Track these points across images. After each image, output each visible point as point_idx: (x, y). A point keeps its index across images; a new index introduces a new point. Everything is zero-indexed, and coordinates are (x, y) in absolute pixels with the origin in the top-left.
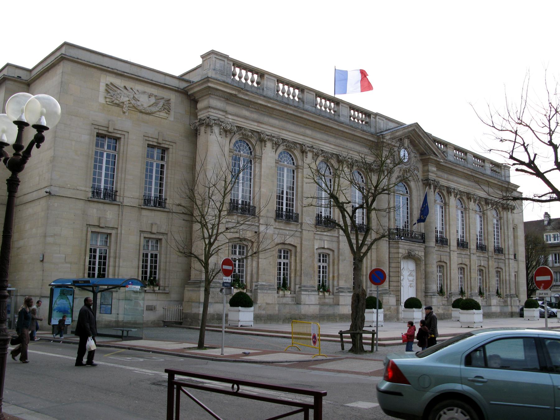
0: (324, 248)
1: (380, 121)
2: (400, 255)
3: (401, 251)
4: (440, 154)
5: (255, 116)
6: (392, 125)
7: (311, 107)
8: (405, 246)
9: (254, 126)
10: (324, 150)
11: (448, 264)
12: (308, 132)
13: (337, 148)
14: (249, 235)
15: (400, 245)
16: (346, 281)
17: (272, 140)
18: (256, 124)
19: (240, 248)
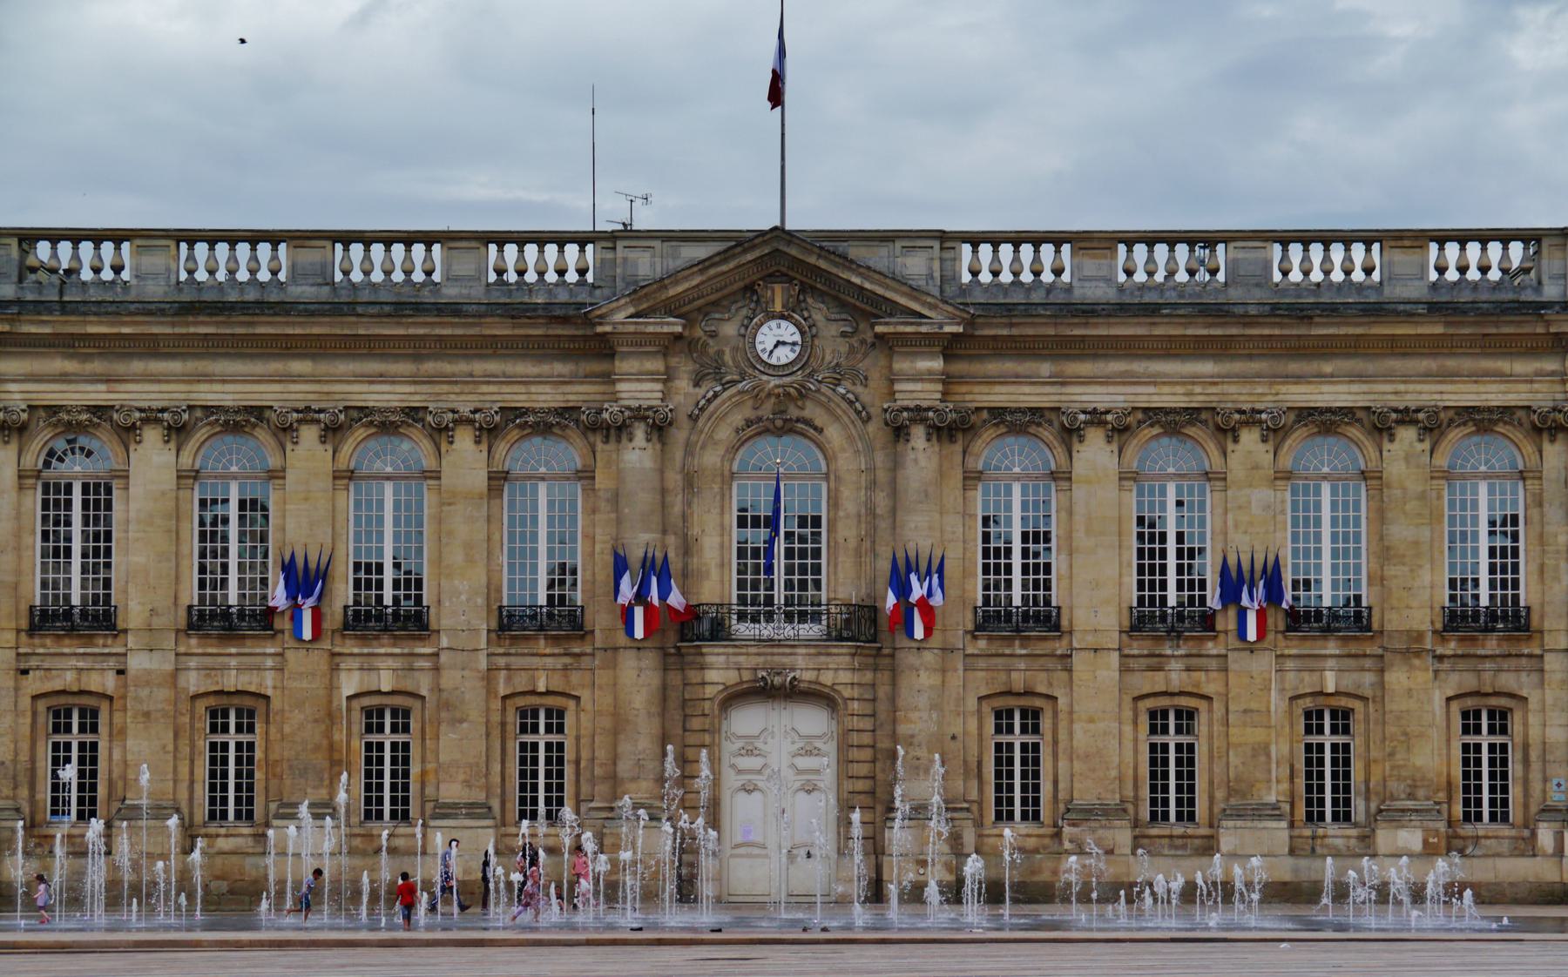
0: (379, 692)
1: (632, 255)
2: (710, 691)
3: (712, 675)
4: (932, 307)
5: (97, 366)
6: (701, 252)
7: (313, 289)
8: (742, 659)
9: (97, 394)
10: (371, 404)
12: (299, 366)
13: (419, 388)
14: (94, 682)
15: (709, 659)
16: (467, 784)
17: (158, 421)
18: (102, 387)
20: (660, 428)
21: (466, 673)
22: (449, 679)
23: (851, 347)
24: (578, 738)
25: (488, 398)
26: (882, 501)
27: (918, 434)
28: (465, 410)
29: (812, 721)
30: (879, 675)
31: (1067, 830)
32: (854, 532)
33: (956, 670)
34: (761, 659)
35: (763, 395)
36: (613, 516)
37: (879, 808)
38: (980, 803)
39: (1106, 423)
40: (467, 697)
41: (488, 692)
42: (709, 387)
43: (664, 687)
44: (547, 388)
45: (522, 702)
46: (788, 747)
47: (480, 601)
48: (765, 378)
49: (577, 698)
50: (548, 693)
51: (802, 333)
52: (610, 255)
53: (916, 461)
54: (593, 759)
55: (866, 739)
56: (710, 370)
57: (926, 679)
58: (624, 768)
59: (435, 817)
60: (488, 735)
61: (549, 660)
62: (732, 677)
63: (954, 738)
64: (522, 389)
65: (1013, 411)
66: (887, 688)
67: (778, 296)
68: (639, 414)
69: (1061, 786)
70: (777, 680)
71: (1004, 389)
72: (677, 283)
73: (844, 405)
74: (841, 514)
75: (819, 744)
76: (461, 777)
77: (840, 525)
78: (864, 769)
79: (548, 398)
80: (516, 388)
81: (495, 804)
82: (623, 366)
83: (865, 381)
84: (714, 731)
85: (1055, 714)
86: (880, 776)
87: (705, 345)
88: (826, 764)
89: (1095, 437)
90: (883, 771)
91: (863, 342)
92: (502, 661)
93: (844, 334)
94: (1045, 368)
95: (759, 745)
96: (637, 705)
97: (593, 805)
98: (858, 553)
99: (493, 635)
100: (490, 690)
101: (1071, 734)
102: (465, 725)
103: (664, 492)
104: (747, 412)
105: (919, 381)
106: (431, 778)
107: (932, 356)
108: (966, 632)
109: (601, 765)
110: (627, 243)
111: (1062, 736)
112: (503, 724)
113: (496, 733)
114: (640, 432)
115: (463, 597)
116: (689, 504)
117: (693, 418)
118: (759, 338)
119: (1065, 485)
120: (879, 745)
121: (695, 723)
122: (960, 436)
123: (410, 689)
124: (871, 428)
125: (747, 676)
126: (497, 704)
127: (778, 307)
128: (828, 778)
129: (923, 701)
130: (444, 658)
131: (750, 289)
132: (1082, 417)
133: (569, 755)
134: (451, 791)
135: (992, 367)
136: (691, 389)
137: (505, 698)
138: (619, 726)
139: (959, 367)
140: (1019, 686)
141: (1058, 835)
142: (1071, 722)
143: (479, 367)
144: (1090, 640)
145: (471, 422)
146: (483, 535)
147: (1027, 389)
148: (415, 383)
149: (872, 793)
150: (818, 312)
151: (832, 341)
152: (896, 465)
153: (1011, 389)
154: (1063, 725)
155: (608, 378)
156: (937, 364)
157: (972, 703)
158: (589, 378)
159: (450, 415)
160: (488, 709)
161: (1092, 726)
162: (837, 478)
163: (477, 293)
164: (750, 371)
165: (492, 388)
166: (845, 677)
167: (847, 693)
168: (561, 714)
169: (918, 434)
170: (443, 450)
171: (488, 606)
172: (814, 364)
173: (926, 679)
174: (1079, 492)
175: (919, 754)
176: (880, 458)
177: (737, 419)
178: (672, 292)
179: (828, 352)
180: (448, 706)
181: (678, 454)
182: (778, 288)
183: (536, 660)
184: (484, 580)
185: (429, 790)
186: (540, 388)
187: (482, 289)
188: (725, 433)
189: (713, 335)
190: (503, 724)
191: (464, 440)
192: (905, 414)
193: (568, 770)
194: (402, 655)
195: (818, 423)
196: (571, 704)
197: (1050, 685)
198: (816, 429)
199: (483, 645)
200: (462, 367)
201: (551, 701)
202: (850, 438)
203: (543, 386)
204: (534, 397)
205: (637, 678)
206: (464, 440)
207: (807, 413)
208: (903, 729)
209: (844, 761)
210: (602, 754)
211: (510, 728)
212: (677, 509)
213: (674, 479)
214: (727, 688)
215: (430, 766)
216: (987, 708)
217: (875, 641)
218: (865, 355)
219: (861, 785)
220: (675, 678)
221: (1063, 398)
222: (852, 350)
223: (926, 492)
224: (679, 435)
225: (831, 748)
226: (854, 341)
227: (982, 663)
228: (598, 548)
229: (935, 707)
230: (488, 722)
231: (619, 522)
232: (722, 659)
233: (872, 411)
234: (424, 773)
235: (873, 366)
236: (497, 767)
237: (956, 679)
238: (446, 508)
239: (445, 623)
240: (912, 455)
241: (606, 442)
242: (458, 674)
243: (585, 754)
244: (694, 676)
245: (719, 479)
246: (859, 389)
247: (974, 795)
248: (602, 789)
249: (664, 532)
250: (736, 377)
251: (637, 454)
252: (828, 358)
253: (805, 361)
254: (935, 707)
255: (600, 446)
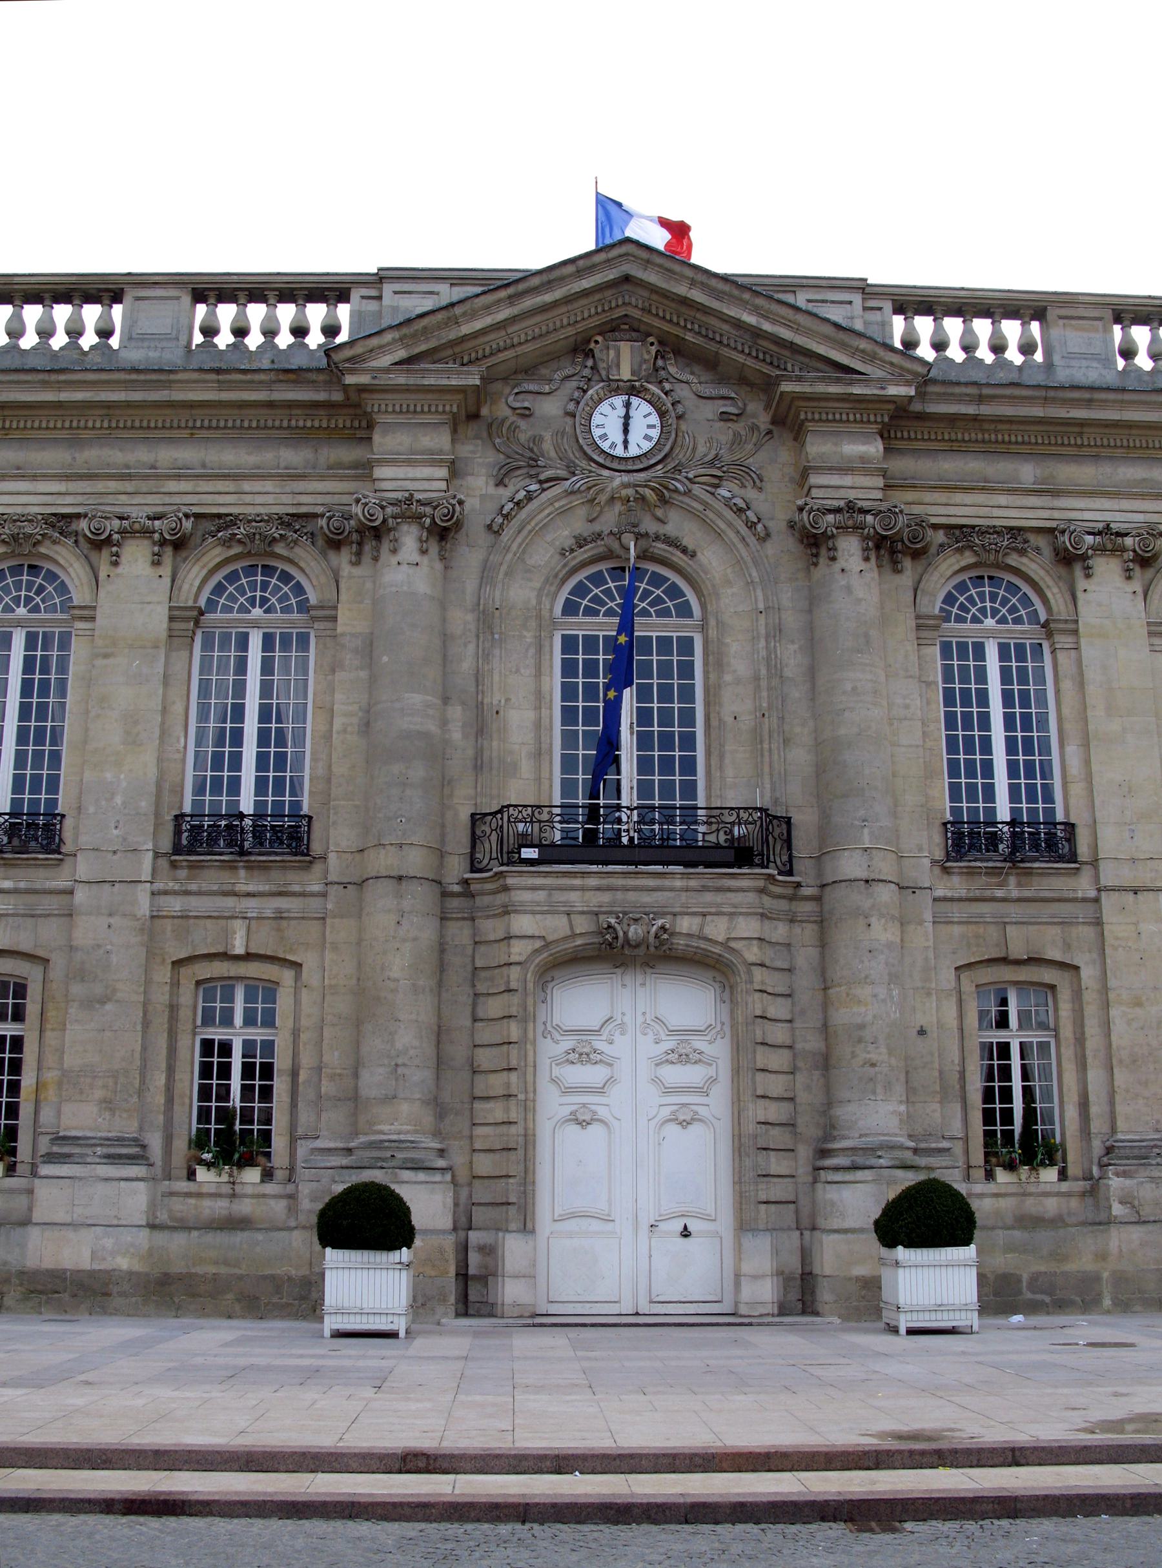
2: (519, 950)
3: (523, 924)
8: (574, 896)
11: (1088, 974)
13: (73, 486)
16: (108, 1105)
19: (250, 997)
20: (443, 531)
21: (112, 920)
22: (88, 930)
23: (736, 435)
24: (296, 1033)
25: (177, 499)
26: (792, 657)
27: (850, 548)
28: (139, 514)
29: (686, 1003)
30: (797, 930)
31: (1115, 1183)
32: (749, 705)
33: (921, 922)
34: (606, 897)
35: (603, 498)
36: (363, 674)
37: (804, 1152)
38: (966, 1140)
39: (1123, 549)
40: (114, 959)
41: (150, 954)
42: (517, 487)
43: (442, 948)
44: (269, 486)
45: (205, 970)
46: (649, 1048)
47: (145, 805)
48: (606, 473)
49: (297, 966)
50: (248, 957)
51: (662, 414)
52: (372, 306)
53: (849, 589)
54: (319, 1069)
55: (779, 1034)
56: (520, 462)
57: (883, 933)
58: (373, 1080)
59: (50, 1158)
60: (146, 1024)
61: (252, 903)
62: (556, 927)
63: (922, 1032)
64: (229, 486)
65: (983, 531)
66: (813, 952)
67: (625, 359)
68: (409, 508)
69: (1094, 1110)
70: (635, 932)
71: (969, 498)
72: (473, 315)
73: (729, 514)
74: (728, 678)
75: (700, 1044)
76: (99, 1094)
77: (727, 695)
78: (776, 1085)
79: (270, 499)
80: (220, 486)
81: (155, 1142)
82: (385, 442)
83: (758, 482)
84: (525, 1018)
85: (1078, 994)
86: (803, 1097)
87: (514, 428)
88: (710, 1075)
89: (1107, 569)
90: (808, 1088)
91: (754, 428)
92: (175, 905)
93: (725, 417)
94: (1027, 472)
95: (600, 1045)
96: (395, 972)
97: (319, 1144)
98: (756, 736)
99: (163, 863)
100: (152, 953)
101: (1107, 1026)
102: (108, 1007)
103: (446, 638)
104: (578, 524)
105: (849, 464)
106: (51, 1094)
107: (865, 438)
108: (934, 862)
109: (332, 1077)
110: (398, 287)
111: (1092, 1029)
112: (173, 1008)
113: (160, 1022)
114: (409, 538)
115: (118, 800)
116: (487, 656)
117: (493, 530)
118: (597, 419)
119: (1063, 640)
120: (799, 1046)
121: (493, 1007)
122: (907, 563)
123: (25, 947)
124: (770, 548)
125: (583, 925)
126: (163, 974)
127: (626, 374)
128: (718, 1104)
129: (877, 967)
130: (81, 895)
131: (581, 348)
132: (1089, 539)
133: (281, 1062)
134: (81, 1117)
135: (950, 466)
136: (491, 490)
137: (178, 964)
138: (366, 1004)
139: (902, 465)
140: (1017, 950)
141: (1093, 1190)
142: (1106, 1005)
143: (167, 455)
144: (1126, 875)
145: (147, 532)
146: (156, 703)
147: (1002, 500)
148: (67, 477)
149: (790, 1125)
150: (688, 385)
151: (706, 430)
152: (813, 601)
153: (980, 498)
154: (1091, 1011)
155: (364, 470)
156: (874, 448)
157: (947, 977)
158: (334, 470)
159: (116, 523)
160: (148, 982)
161: (1138, 1010)
162: (720, 624)
163: (172, 356)
164: (584, 463)
165: (184, 486)
166: (748, 927)
167: (752, 953)
168: (271, 994)
169: (850, 548)
170: (102, 575)
171: (157, 815)
172: (680, 456)
173: (883, 933)
174: (1090, 651)
175: (873, 1057)
176: (787, 596)
177: (563, 534)
178: (466, 329)
179: (701, 441)
180: (80, 974)
181: (471, 585)
182: (625, 348)
183: (230, 902)
184: (152, 773)
185: (47, 1116)
186: (257, 486)
187: (181, 352)
188: (543, 556)
189: (526, 414)
190: (173, 1008)
191: (136, 558)
192: (830, 518)
193: (280, 1085)
194: (16, 891)
195: (687, 542)
196: (287, 976)
197: (1067, 946)
198: (684, 551)
199: (146, 875)
200: (140, 455)
201: (253, 969)
202: (739, 562)
203: (260, 481)
204: (248, 499)
205: (398, 933)
206: (136, 558)
207: (670, 529)
208: (842, 1016)
209: (744, 1069)
210: (334, 1058)
211: (184, 1014)
212: (467, 665)
213: (462, 620)
214: (547, 945)
215: (50, 1076)
216: (968, 987)
217: (790, 873)
218: (758, 447)
219: (775, 1111)
220: (460, 933)
221: (1056, 514)
222: (737, 440)
223: (866, 635)
224: (470, 555)
225: (719, 1050)
226: (740, 427)
227: (957, 912)
228: (338, 724)
229: (894, 978)
230: (145, 1005)
231: (373, 680)
232: (541, 896)
233: (770, 524)
234: (39, 1087)
235: (775, 461)
236: (160, 1079)
237: (923, 936)
238: (100, 662)
239: (85, 840)
240: (842, 581)
241: (357, 563)
242: (104, 921)
243: (307, 1060)
244: (492, 928)
245: (533, 624)
246: (751, 494)
247: (956, 1128)
248: (334, 1118)
249: (446, 700)
250: (562, 473)
251: (407, 567)
252: (701, 449)
253: (664, 453)
254: (894, 978)
255: (346, 570)
